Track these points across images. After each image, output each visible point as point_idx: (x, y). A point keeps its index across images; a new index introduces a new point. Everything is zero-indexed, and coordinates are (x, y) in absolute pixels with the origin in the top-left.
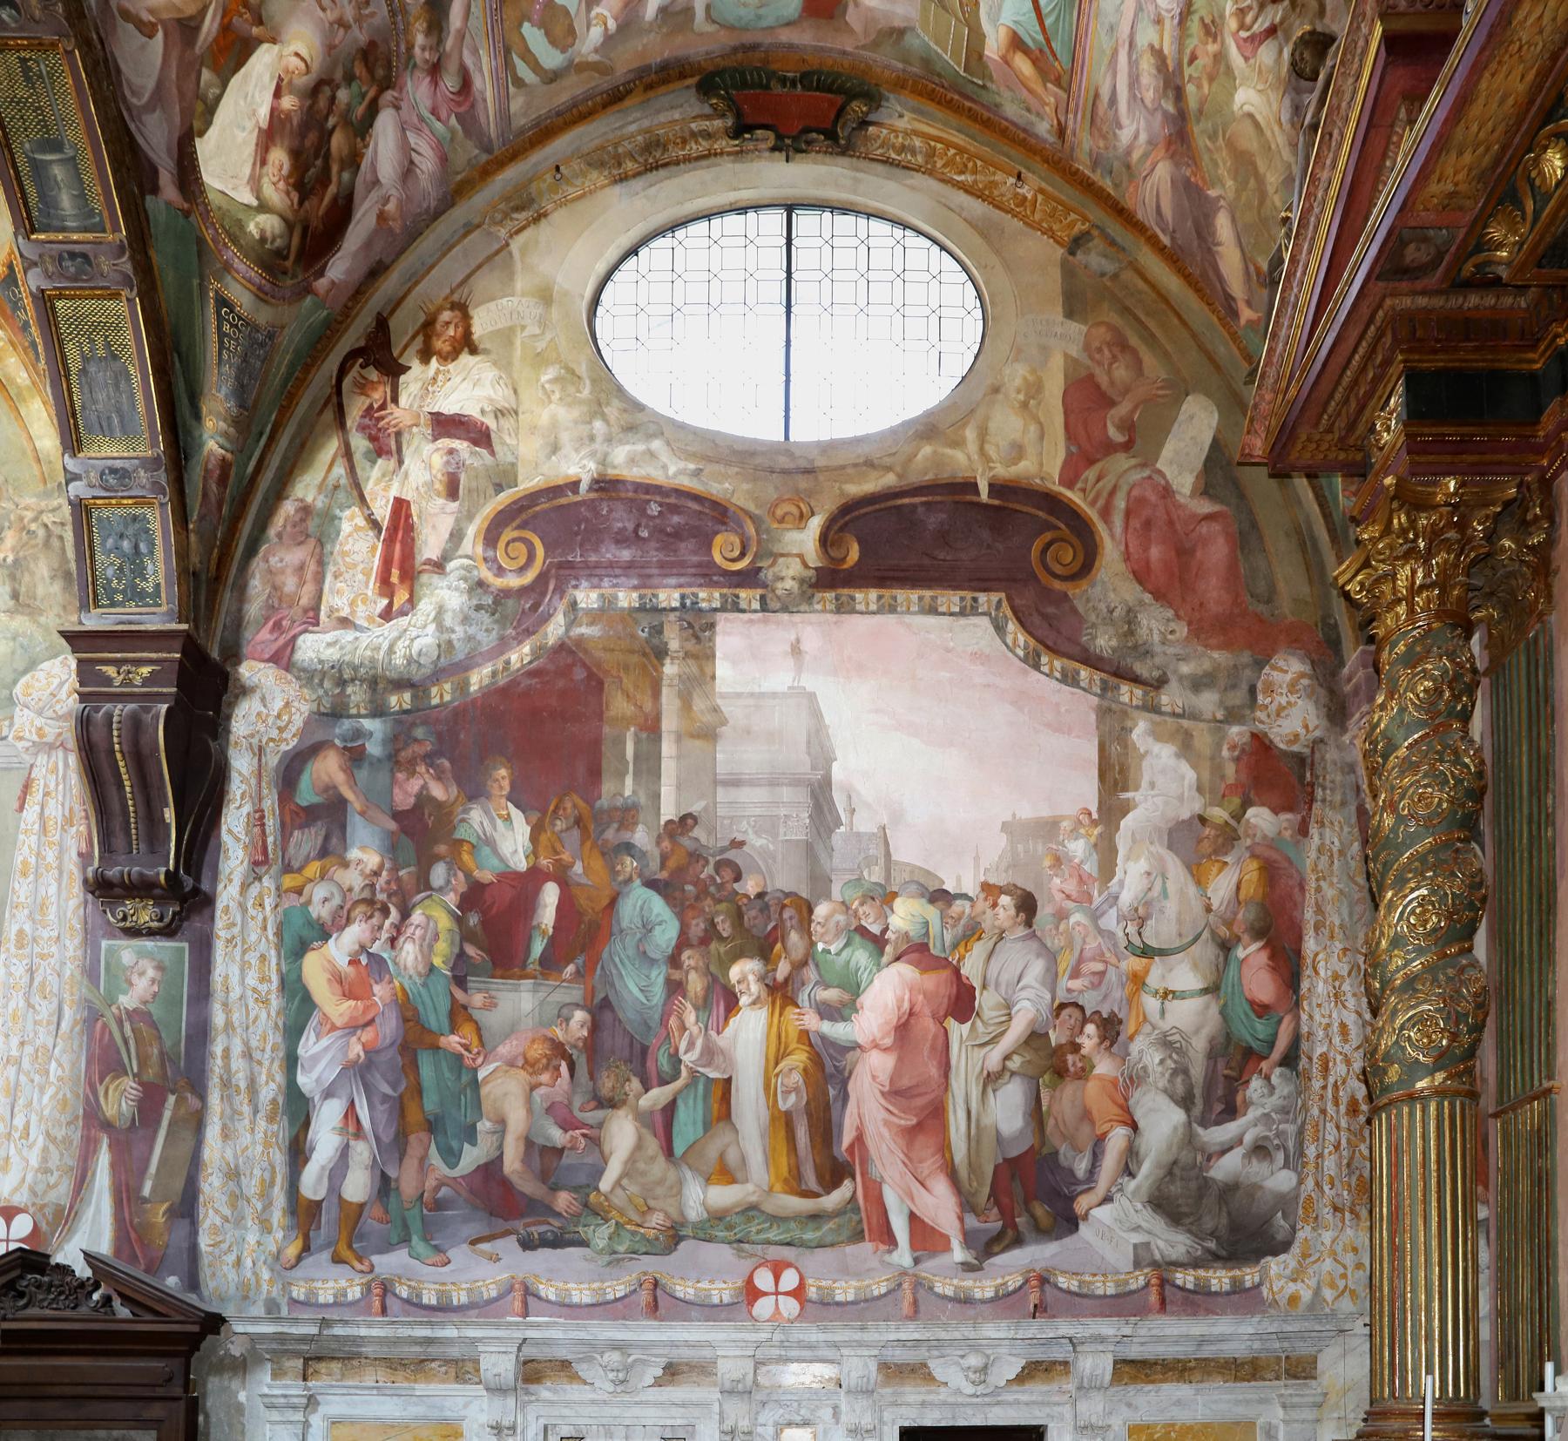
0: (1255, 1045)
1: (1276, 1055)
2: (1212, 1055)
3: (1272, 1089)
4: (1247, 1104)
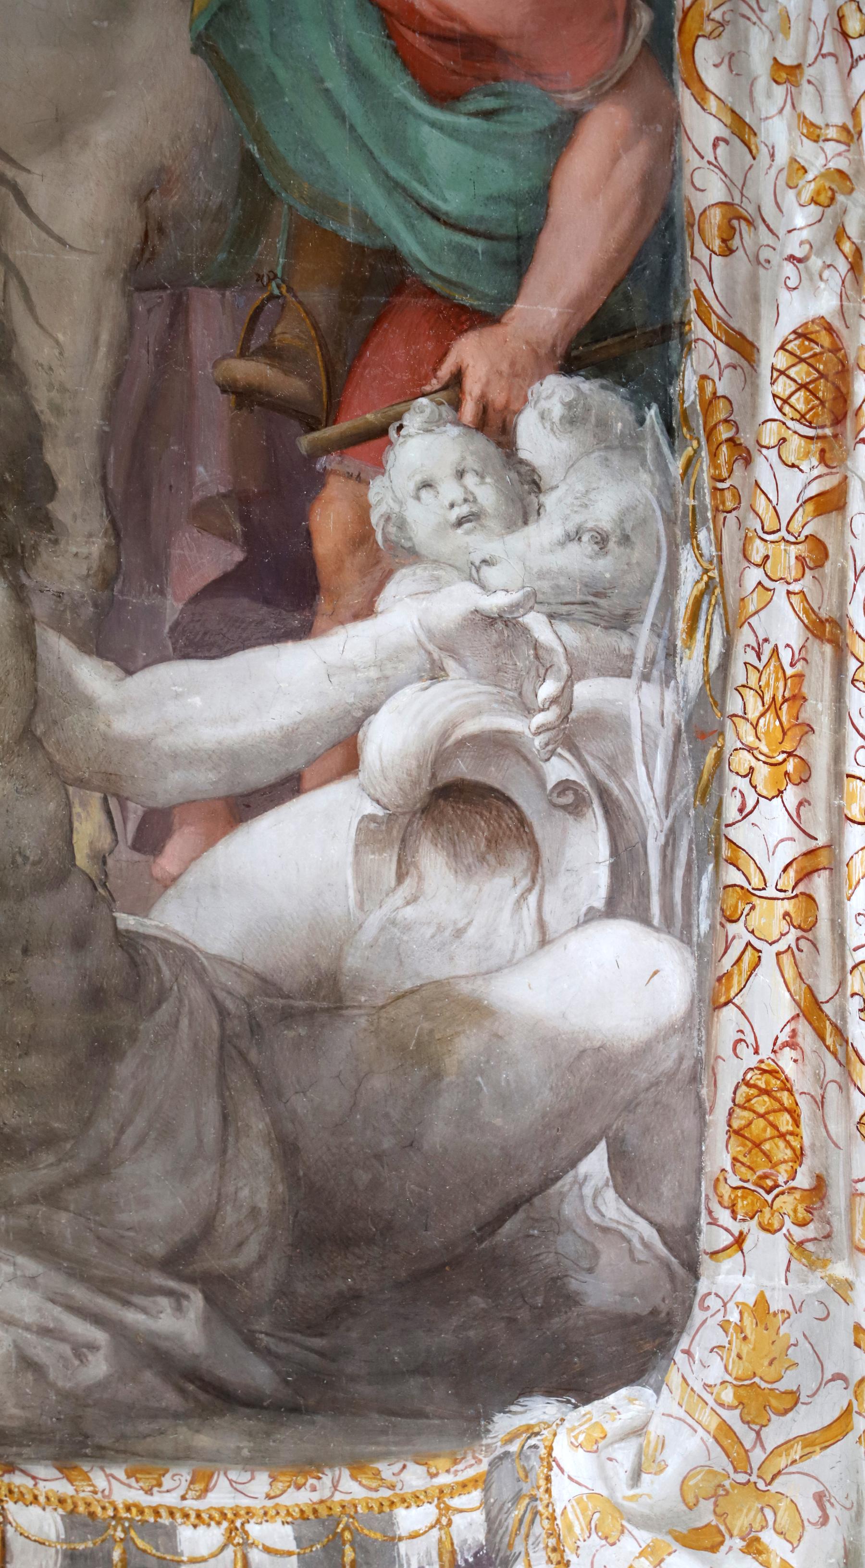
0: (418, 243)
1: (546, 305)
2: (154, 269)
3: (526, 490)
4: (379, 557)
